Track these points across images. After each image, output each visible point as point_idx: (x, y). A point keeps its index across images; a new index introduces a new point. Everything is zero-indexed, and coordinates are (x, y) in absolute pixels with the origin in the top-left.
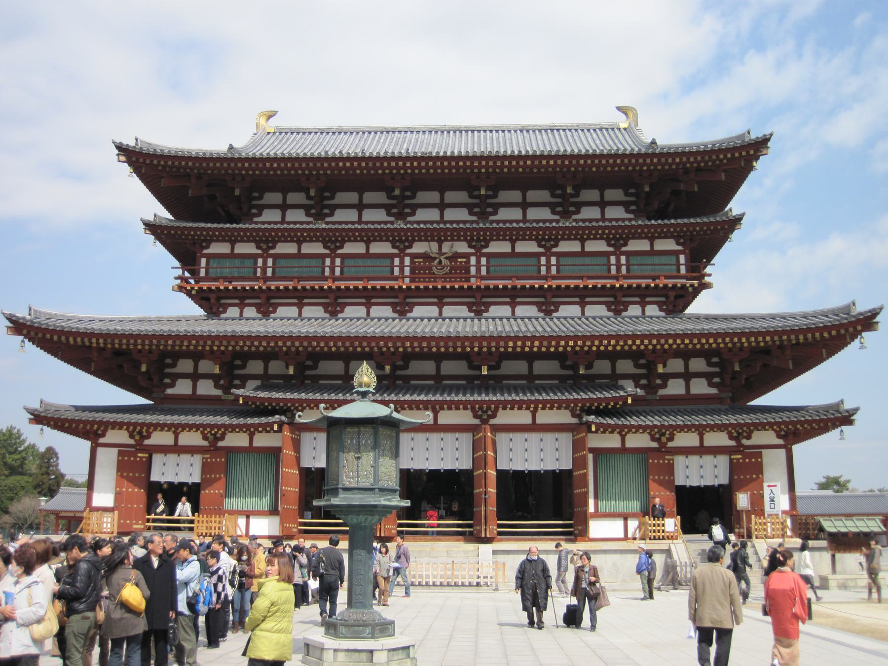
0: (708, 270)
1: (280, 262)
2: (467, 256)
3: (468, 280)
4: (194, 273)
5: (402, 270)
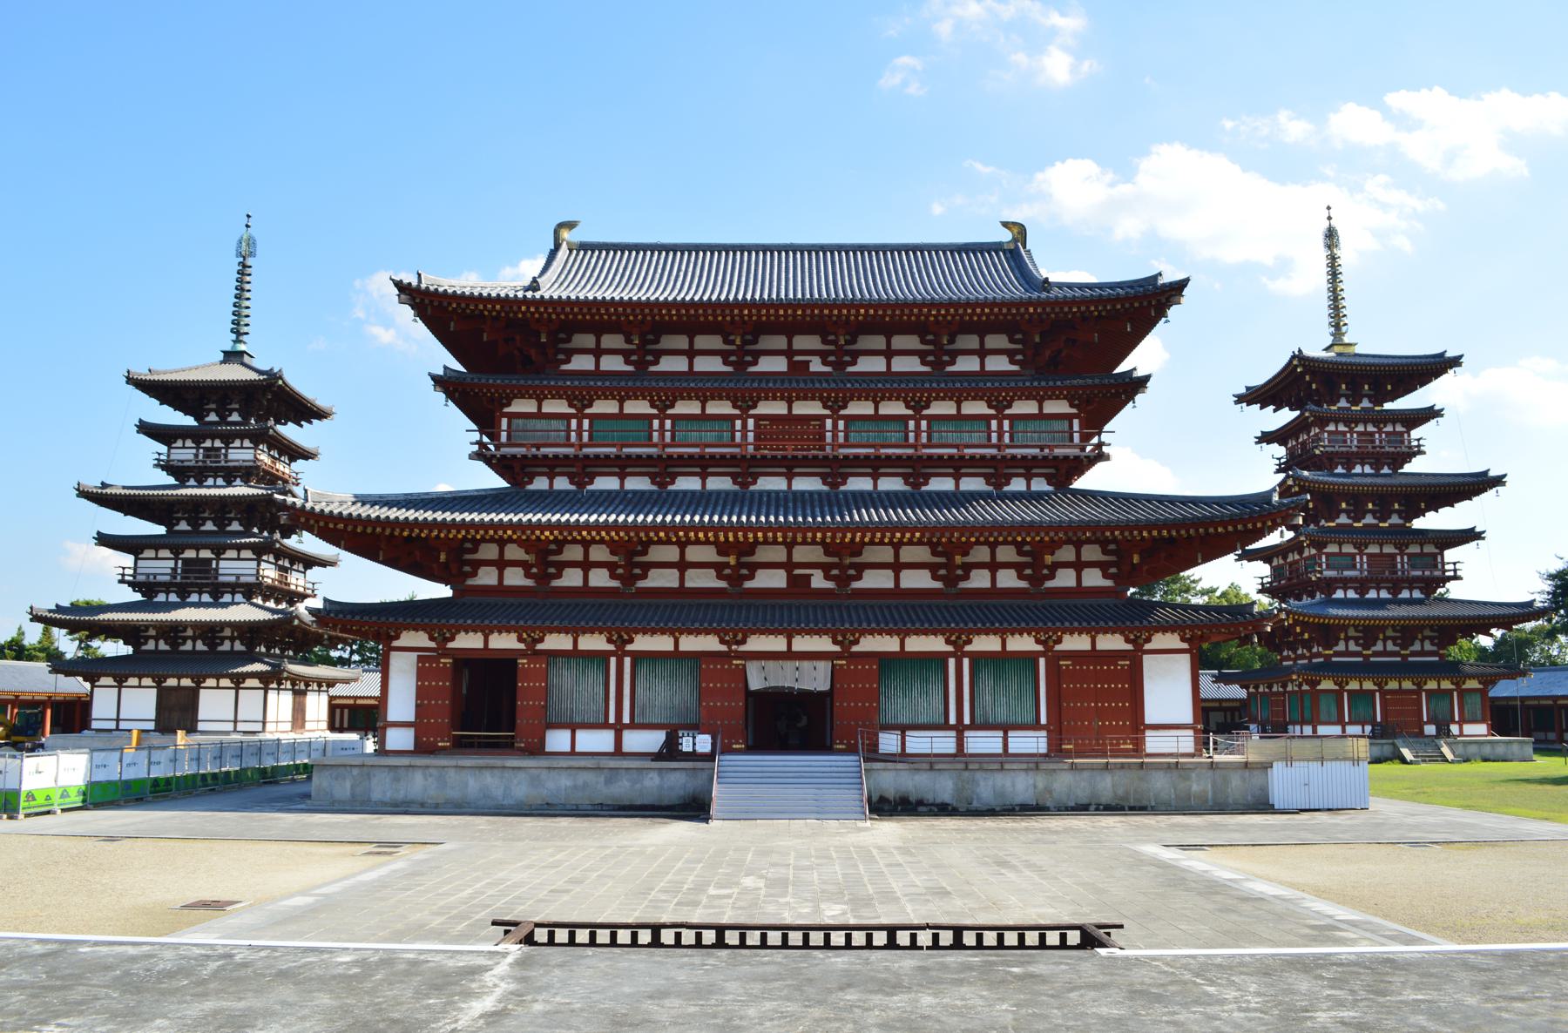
0: (1104, 438)
1: (598, 425)
2: (821, 418)
3: (822, 448)
4: (494, 437)
5: (744, 437)
